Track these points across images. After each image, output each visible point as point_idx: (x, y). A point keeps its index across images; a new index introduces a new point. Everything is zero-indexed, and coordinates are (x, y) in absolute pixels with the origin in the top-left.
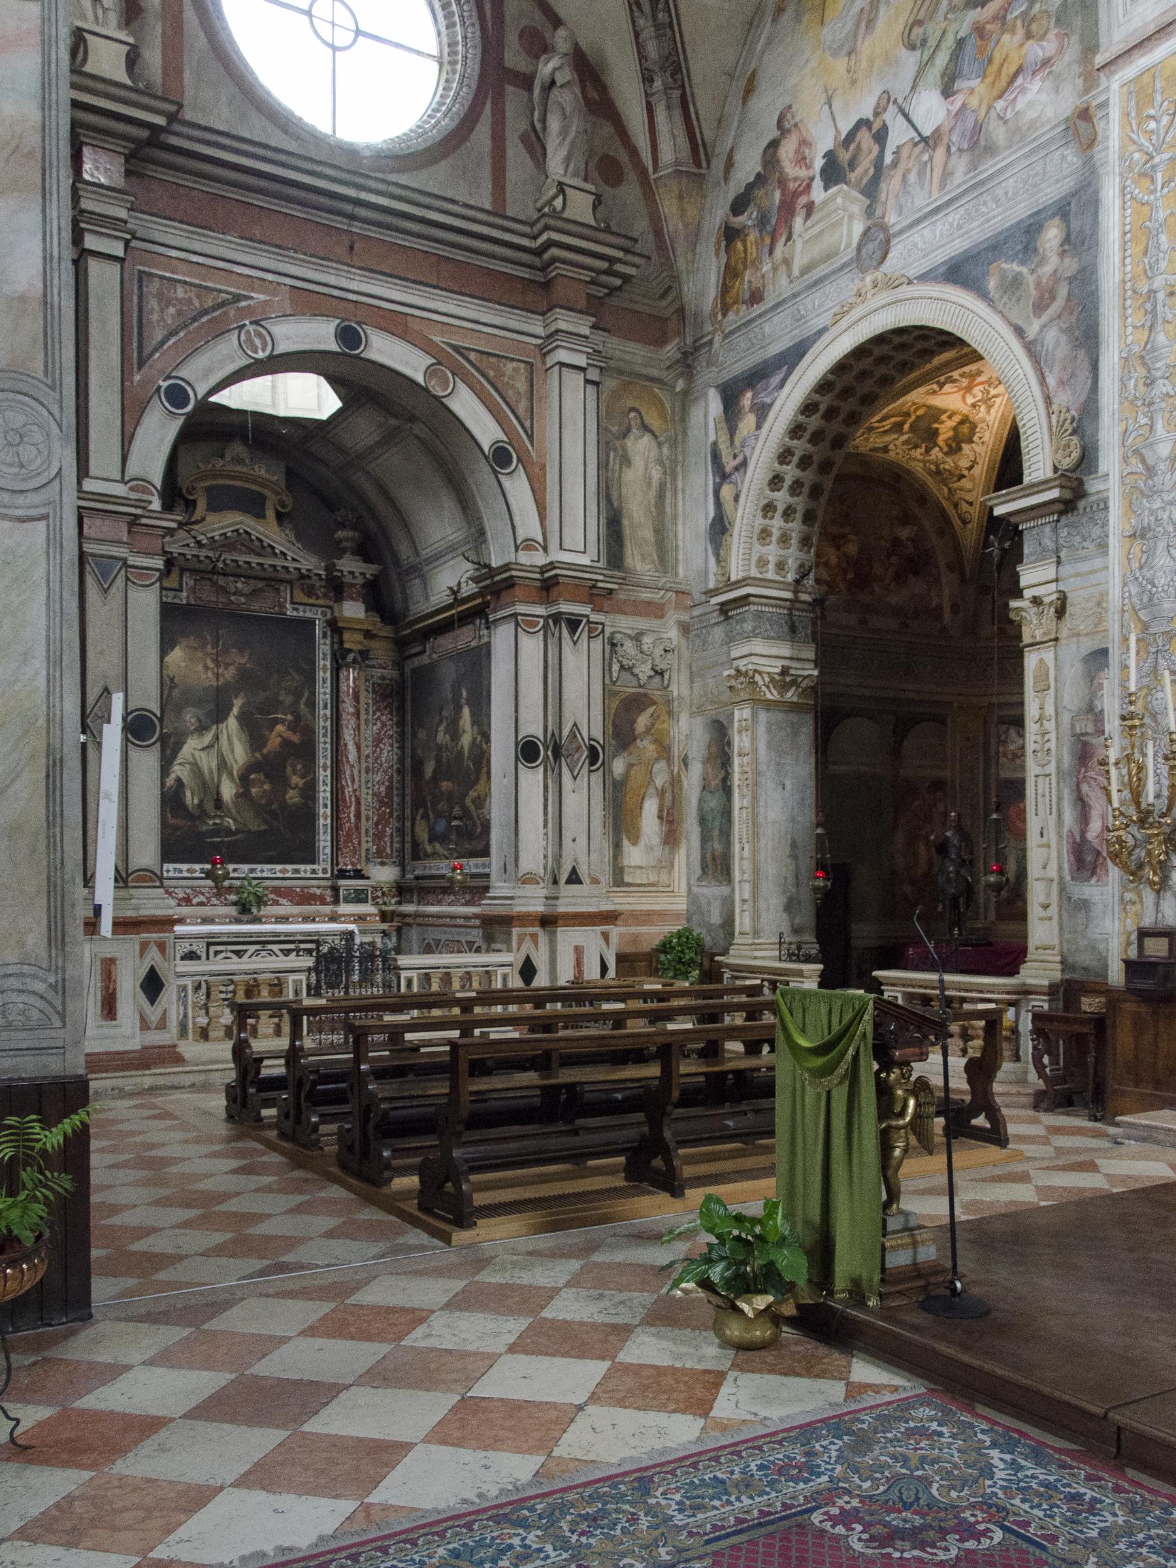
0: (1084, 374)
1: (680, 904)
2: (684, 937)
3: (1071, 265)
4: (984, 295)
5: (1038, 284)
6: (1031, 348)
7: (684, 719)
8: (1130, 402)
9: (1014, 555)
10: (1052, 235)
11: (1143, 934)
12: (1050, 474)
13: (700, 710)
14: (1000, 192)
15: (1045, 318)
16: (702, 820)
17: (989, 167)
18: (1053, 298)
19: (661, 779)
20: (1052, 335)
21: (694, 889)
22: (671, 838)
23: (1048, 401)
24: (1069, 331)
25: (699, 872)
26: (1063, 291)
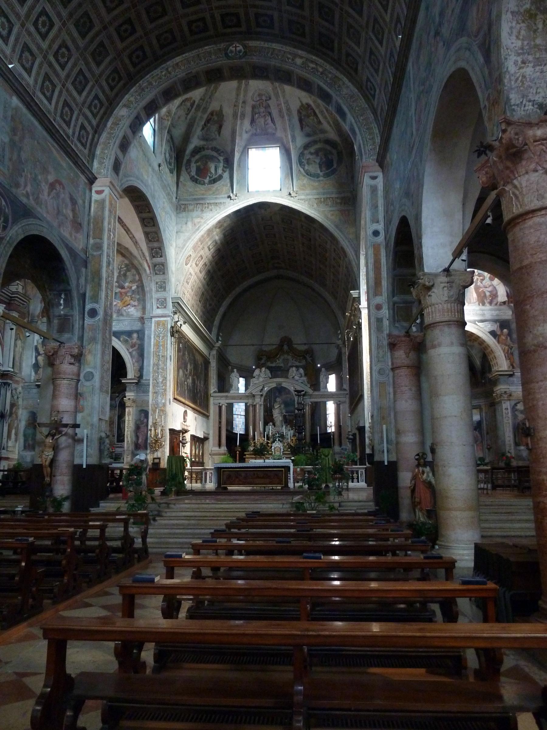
0: (141, 362)
1: (16, 456)
2: (19, 464)
3: (138, 342)
4: (120, 340)
5: (132, 342)
6: (130, 353)
7: (21, 410)
8: (154, 371)
9: (125, 390)
10: (135, 335)
11: (154, 459)
12: (133, 377)
13: (26, 408)
14: (124, 323)
15: (133, 349)
16: (25, 435)
17: (121, 318)
18: (135, 346)
19: (15, 425)
20: (134, 353)
21: (21, 453)
22: (16, 440)
23: (133, 364)
24: (138, 353)
25: (23, 448)
26: (137, 346)
